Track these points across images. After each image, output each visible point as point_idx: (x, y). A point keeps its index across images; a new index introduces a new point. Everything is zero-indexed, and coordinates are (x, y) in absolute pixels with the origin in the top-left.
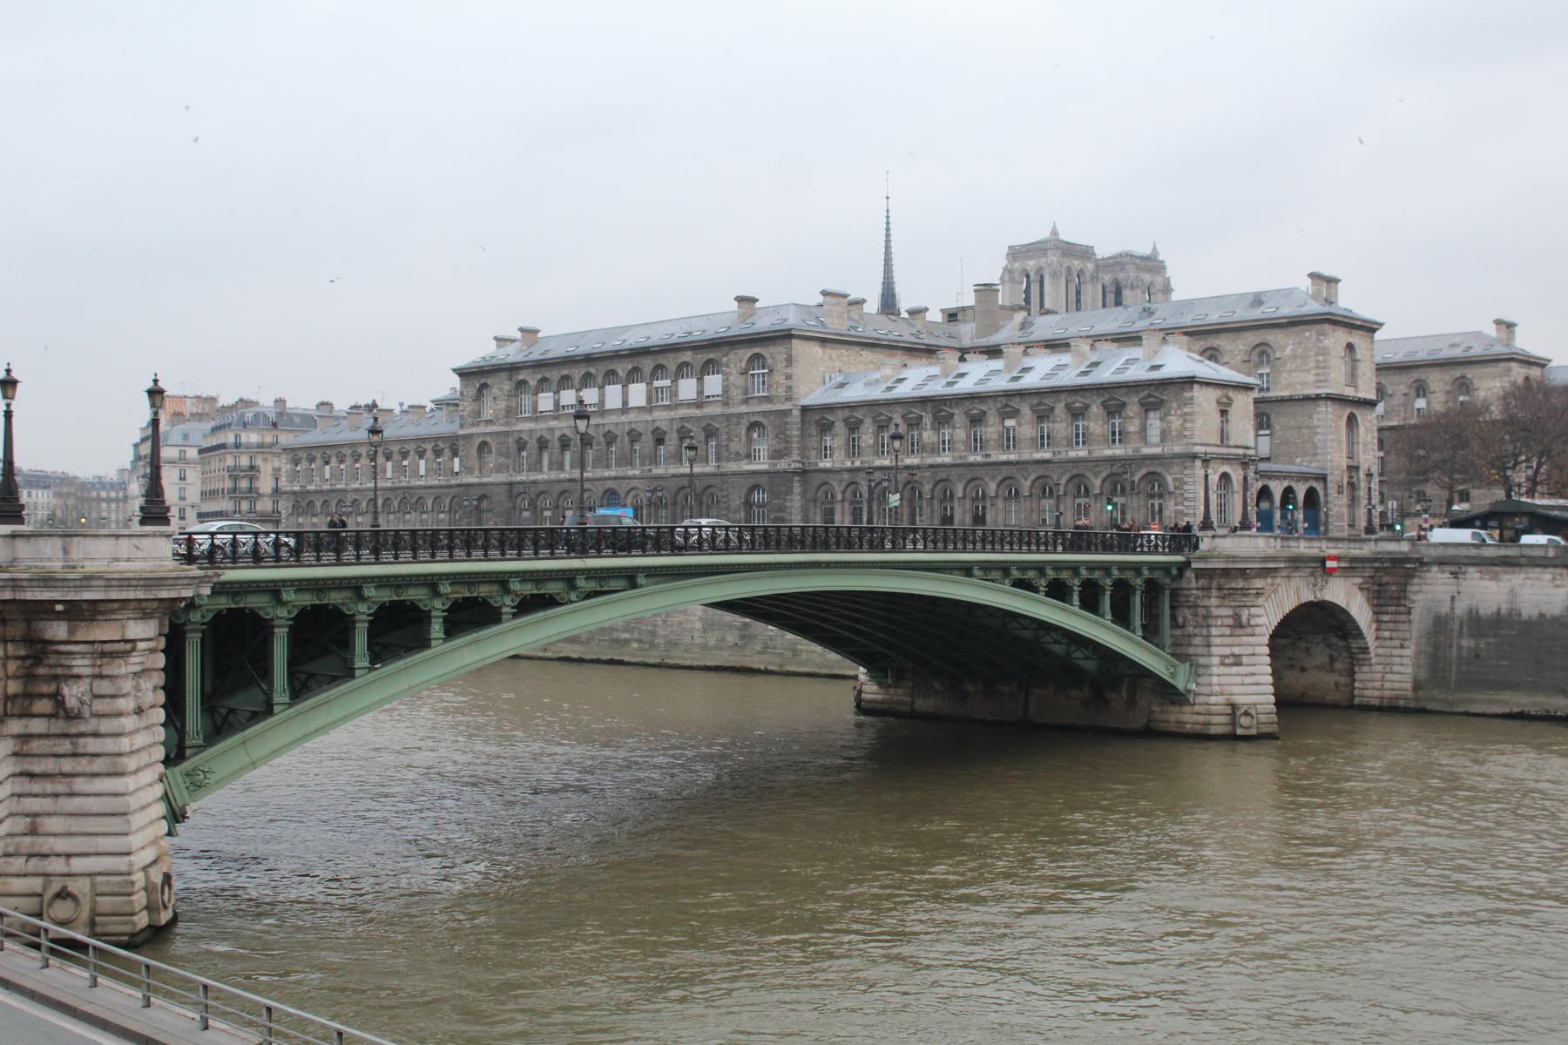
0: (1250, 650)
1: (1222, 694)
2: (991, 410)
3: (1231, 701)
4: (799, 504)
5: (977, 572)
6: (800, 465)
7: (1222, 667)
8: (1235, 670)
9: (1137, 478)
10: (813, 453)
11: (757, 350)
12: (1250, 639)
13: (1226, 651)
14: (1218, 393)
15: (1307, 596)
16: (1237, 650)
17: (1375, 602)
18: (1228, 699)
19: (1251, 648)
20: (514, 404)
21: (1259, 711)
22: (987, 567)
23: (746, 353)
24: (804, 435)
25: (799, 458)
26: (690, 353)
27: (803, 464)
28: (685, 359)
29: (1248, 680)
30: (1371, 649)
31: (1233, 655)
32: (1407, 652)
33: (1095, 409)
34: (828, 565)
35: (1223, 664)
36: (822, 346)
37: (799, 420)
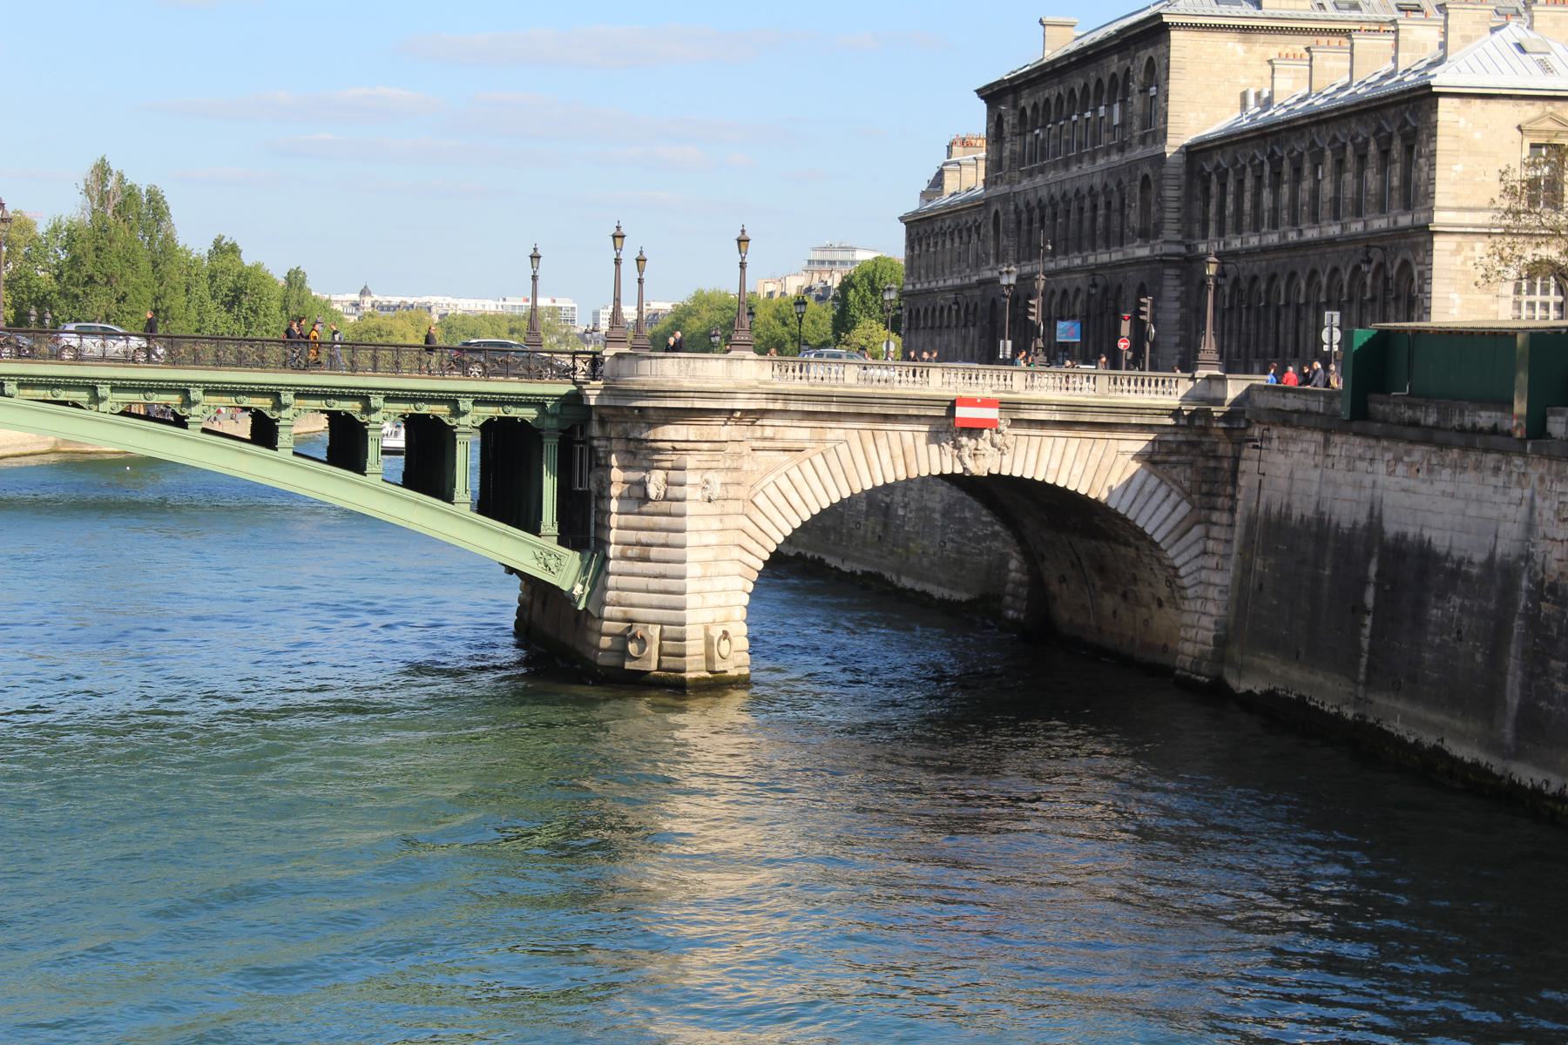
0: (660, 537)
1: (620, 605)
2: (1301, 146)
4: (1178, 316)
6: (1183, 249)
9: (1394, 272)
10: (1197, 228)
11: (1150, 52)
12: (663, 521)
13: (631, 536)
14: (1532, 111)
15: (938, 460)
16: (644, 536)
17: (1204, 488)
18: (625, 612)
19: (665, 534)
20: (1018, 148)
21: (666, 635)
22: (25, 383)
23: (1144, 55)
24: (1188, 198)
25: (1179, 237)
26: (1115, 57)
27: (1188, 247)
28: (1114, 69)
30: (1182, 572)
31: (639, 544)
32: (1216, 578)
33: (1372, 148)
35: (624, 558)
36: (1243, 41)
37: (1181, 171)
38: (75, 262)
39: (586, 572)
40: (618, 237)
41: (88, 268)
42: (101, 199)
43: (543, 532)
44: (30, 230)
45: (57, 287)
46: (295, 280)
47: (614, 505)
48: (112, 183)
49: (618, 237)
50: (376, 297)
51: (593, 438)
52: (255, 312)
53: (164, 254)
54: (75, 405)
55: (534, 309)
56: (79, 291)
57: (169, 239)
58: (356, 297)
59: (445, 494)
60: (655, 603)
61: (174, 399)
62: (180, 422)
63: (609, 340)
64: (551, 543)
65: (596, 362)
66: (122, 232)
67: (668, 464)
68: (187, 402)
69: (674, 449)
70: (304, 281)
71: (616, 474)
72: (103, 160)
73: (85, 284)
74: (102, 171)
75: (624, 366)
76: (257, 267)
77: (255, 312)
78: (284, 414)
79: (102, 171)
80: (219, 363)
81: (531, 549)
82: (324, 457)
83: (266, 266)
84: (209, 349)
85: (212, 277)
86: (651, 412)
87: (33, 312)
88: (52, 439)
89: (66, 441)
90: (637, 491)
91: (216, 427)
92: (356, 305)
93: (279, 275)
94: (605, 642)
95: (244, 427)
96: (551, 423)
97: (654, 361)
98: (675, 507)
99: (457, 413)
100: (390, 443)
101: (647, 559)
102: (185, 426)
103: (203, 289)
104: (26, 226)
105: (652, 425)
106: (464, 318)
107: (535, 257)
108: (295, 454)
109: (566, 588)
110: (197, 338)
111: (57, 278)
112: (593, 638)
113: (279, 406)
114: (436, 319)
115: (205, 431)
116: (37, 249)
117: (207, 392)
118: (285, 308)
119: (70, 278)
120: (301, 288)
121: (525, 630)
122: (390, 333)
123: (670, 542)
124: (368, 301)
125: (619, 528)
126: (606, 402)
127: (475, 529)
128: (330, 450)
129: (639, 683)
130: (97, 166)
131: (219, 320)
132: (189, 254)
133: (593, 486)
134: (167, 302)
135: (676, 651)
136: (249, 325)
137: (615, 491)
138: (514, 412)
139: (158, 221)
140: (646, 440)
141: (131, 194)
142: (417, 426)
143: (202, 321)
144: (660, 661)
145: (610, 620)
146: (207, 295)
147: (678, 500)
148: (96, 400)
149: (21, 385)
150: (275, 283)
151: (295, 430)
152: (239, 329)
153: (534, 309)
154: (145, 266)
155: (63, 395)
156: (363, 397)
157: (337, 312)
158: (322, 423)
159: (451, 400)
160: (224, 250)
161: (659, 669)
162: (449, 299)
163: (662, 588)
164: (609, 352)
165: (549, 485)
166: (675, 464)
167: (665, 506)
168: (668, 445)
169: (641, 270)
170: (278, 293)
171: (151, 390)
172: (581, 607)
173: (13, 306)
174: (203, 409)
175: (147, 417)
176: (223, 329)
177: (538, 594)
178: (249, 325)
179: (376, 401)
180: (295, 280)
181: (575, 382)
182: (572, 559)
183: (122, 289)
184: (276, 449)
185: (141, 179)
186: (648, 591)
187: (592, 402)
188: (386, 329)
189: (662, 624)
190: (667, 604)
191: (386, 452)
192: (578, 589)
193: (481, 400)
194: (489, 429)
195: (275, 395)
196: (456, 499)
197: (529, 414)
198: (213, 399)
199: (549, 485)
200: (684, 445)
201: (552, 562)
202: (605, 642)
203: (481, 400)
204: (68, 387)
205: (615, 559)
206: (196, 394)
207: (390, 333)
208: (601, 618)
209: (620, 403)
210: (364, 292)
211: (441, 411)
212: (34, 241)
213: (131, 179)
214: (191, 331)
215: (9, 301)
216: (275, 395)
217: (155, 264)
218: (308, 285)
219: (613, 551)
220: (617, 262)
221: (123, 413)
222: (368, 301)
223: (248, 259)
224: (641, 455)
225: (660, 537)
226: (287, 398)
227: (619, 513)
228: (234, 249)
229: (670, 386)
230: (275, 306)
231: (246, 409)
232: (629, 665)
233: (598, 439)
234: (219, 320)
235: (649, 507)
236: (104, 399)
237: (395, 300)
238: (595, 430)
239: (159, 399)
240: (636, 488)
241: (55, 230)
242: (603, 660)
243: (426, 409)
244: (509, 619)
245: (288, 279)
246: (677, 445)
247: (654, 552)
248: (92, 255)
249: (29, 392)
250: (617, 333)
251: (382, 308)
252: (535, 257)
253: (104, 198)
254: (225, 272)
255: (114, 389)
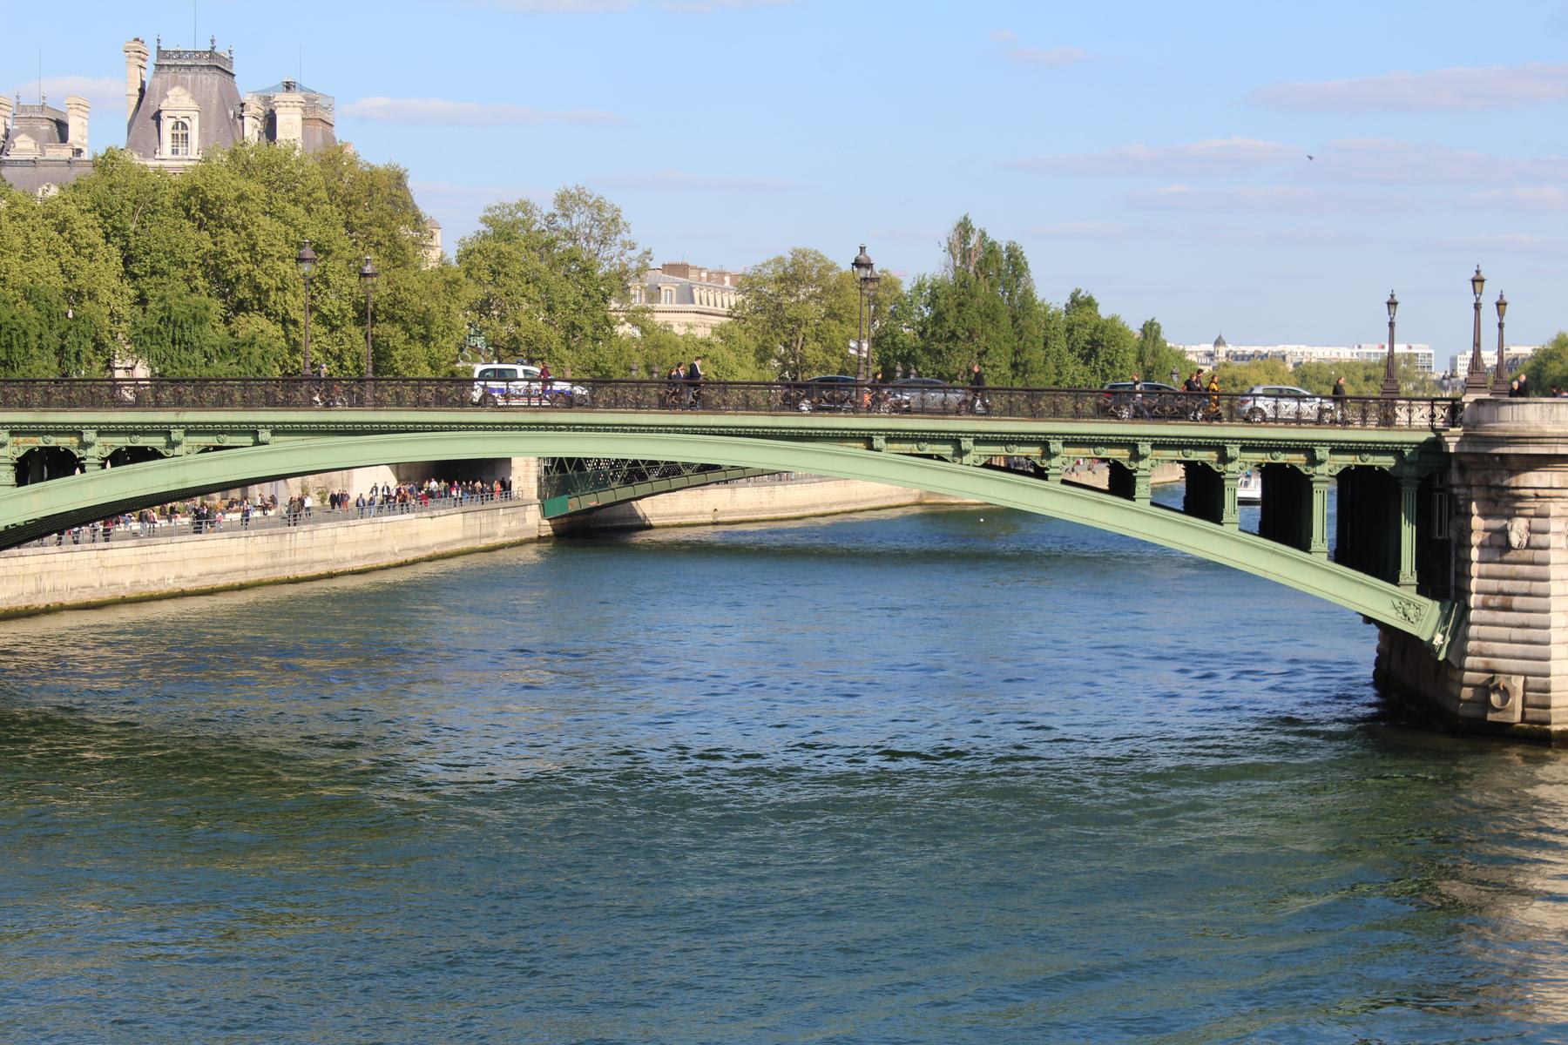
0: (1523, 586)
1: (1481, 654)
3: (1492, 666)
5: (879, 442)
7: (1484, 612)
8: (1501, 616)
12: (1526, 570)
13: (1493, 585)
16: (1506, 585)
18: (1487, 663)
19: (1527, 583)
21: (1530, 686)
22: (893, 437)
29: (1517, 634)
31: (1500, 593)
34: (571, 427)
35: (1485, 607)
38: (939, 318)
39: (1446, 622)
40: (1478, 281)
41: (950, 323)
42: (963, 257)
43: (1402, 580)
44: (895, 288)
45: (921, 343)
46: (1151, 330)
47: (1475, 554)
48: (974, 240)
49: (1478, 281)
50: (1230, 347)
51: (1453, 486)
52: (1111, 364)
53: (1025, 307)
54: (940, 458)
55: (1391, 355)
56: (942, 347)
57: (1028, 293)
58: (1210, 347)
59: (1304, 545)
60: (1518, 653)
61: (1035, 451)
62: (1040, 474)
63: (1469, 386)
64: (1410, 593)
65: (1455, 408)
66: (983, 289)
67: (1531, 512)
68: (1048, 454)
69: (1537, 496)
70: (1158, 332)
71: (1477, 523)
72: (966, 218)
73: (950, 339)
74: (964, 229)
75: (1484, 412)
76: (1114, 320)
77: (1111, 364)
78: (1142, 464)
79: (964, 229)
80: (1077, 415)
81: (1390, 598)
82: (1180, 506)
83: (1123, 319)
84: (1068, 403)
85: (1070, 330)
86: (1513, 459)
87: (899, 368)
88: (916, 491)
89: (930, 494)
90: (1499, 540)
91: (1074, 478)
92: (1210, 355)
93: (1135, 327)
94: (1467, 693)
95: (1102, 478)
96: (1409, 471)
97: (1515, 407)
98: (1539, 555)
99: (1313, 461)
100: (1243, 493)
101: (1507, 608)
102: (1045, 477)
103: (1061, 344)
104: (892, 285)
105: (1514, 472)
106: (1319, 366)
107: (1392, 304)
108: (1152, 504)
109: (1425, 638)
110: (1056, 391)
111: (921, 334)
112: (1455, 689)
113: (1136, 457)
114: (1290, 367)
115: (1064, 482)
116: (902, 308)
117: (1066, 444)
118: (1140, 359)
119: (933, 334)
120: (1156, 338)
121: (1383, 677)
122: (1245, 383)
123: (1533, 591)
124: (1222, 351)
125: (1480, 577)
126: (1466, 449)
127: (1331, 578)
128: (1186, 500)
129: (1505, 735)
130: (960, 224)
131: (1075, 372)
132: (1047, 308)
133: (1453, 535)
134: (1027, 356)
135: (1541, 702)
136: (1106, 377)
137: (1476, 539)
138: (1372, 460)
139: (1017, 277)
140: (1509, 488)
141: (992, 249)
142: (1270, 474)
143: (1059, 374)
144: (1523, 713)
145: (1471, 670)
146: (1064, 348)
147: (1541, 548)
148: (960, 453)
149: (889, 440)
150: (1131, 335)
151: (1152, 480)
152: (1096, 382)
153: (1391, 355)
154: (1005, 321)
155: (929, 449)
156: (1219, 447)
157: (1192, 363)
158: (1180, 471)
159: (1307, 449)
160: (1081, 303)
161: (1523, 720)
162: (1303, 348)
163: (1525, 638)
164: (1469, 398)
165: (1408, 534)
166: (1538, 512)
167: (1528, 554)
168: (1530, 492)
169: (1501, 314)
170: (1133, 344)
171: (1012, 442)
172: (1441, 657)
173: (879, 363)
174: (1063, 460)
175: (1007, 469)
176: (1080, 381)
177: (1396, 644)
178: (1106, 377)
179: (1233, 451)
180: (1151, 330)
181: (1433, 429)
182: (1432, 609)
183: (982, 341)
184: (1134, 500)
185: (1001, 237)
186: (1511, 641)
187: (1452, 450)
188: (1240, 379)
189: (1526, 675)
190: (1531, 654)
191: (1244, 502)
192: (1438, 639)
193: (1338, 448)
194: (1346, 478)
195: (1133, 446)
196: (1313, 548)
197: (1387, 462)
198: (1072, 451)
199: (1408, 534)
200: (1547, 492)
201: (1411, 612)
202: (1467, 693)
203: (1338, 448)
204: (933, 441)
205: (1476, 608)
206: (1055, 446)
207: (1245, 383)
208: (1462, 669)
209: (1481, 450)
210: (1219, 342)
211: (1298, 460)
212: (899, 300)
213: (992, 236)
214: (1049, 383)
215: (876, 357)
216: (1133, 446)
217: (1015, 319)
218: (1163, 336)
219: (1474, 600)
220: (1477, 307)
221: (985, 466)
222: (1222, 351)
223: (1104, 312)
224: (1503, 503)
225: (1523, 586)
226: (1144, 448)
227: (1480, 562)
228: (1090, 302)
229: (1532, 431)
230: (1132, 357)
231: (1104, 460)
232: (1491, 717)
233: (1458, 486)
234: (1075, 372)
235: (1511, 556)
236: (967, 452)
237: (1250, 350)
238: (1455, 478)
239: (1019, 451)
240: (1497, 536)
241: (920, 288)
242: (1464, 712)
243: (1282, 458)
244: (1368, 671)
245: (1143, 331)
246: (1540, 492)
247: (1517, 602)
248: (953, 313)
249: (896, 446)
250: (1477, 379)
251: (1236, 358)
252: (1392, 304)
253: (966, 255)
254: (1084, 324)
255: (977, 442)
